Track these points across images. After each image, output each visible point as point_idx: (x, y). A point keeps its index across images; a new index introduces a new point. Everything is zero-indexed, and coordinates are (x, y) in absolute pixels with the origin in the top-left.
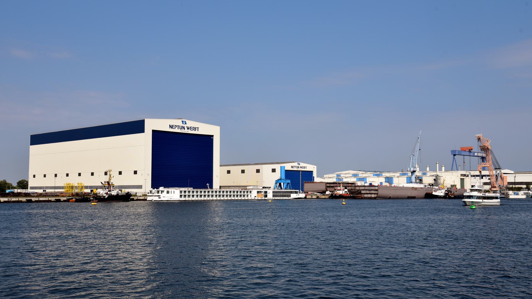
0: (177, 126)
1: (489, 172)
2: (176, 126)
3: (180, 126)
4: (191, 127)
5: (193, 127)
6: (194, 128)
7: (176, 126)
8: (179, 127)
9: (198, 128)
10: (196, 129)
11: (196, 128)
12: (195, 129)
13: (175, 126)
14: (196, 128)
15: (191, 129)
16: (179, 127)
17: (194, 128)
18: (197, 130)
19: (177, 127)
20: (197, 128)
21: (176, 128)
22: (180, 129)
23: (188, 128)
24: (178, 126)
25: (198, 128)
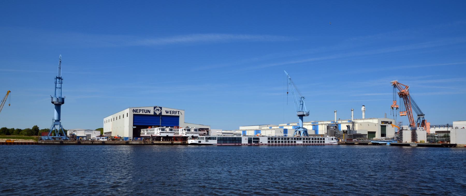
0: (142, 110)
1: (61, 96)
2: (140, 110)
3: (145, 110)
4: (170, 111)
5: (173, 111)
6: (174, 112)
7: (140, 110)
8: (144, 111)
10: (176, 113)
11: (177, 112)
12: (175, 113)
14: (176, 111)
15: (170, 112)
16: (144, 111)
17: (174, 112)
19: (141, 111)
20: (177, 112)
21: (140, 112)
22: (145, 112)
24: (143, 110)
25: (179, 112)
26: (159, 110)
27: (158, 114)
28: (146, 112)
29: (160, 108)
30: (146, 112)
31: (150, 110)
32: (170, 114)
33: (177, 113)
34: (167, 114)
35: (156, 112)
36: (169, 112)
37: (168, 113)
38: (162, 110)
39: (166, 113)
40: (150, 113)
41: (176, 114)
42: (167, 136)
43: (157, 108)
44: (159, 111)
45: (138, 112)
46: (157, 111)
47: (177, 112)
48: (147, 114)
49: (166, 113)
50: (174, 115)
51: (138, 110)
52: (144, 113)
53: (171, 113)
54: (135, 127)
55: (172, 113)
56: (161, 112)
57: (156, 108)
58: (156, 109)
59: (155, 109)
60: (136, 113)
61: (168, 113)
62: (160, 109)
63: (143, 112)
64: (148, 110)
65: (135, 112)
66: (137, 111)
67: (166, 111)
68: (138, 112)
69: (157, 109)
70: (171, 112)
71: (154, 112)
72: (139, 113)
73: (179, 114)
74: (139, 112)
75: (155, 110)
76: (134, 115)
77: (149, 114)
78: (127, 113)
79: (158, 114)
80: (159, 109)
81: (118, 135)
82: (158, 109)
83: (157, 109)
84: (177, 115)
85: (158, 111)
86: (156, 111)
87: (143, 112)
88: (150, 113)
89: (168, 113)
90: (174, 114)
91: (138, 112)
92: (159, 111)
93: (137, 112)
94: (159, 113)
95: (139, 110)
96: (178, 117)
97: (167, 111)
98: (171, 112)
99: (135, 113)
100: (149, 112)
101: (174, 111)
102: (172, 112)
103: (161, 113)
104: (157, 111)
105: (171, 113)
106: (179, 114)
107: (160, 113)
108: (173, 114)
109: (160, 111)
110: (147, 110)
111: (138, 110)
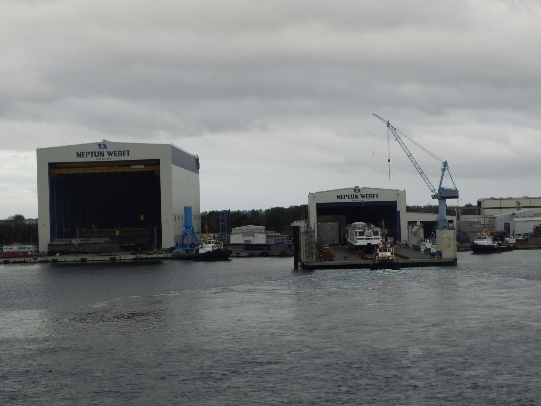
0: (91, 153)
9: (128, 151)
11: (125, 152)
14: (124, 151)
15: (115, 154)
17: (120, 152)
18: (126, 155)
21: (87, 155)
23: (110, 154)
25: (128, 151)
37: (111, 156)
49: (109, 156)
54: (304, 219)
61: (111, 155)
89: (111, 156)
101: (121, 151)
102: (117, 152)
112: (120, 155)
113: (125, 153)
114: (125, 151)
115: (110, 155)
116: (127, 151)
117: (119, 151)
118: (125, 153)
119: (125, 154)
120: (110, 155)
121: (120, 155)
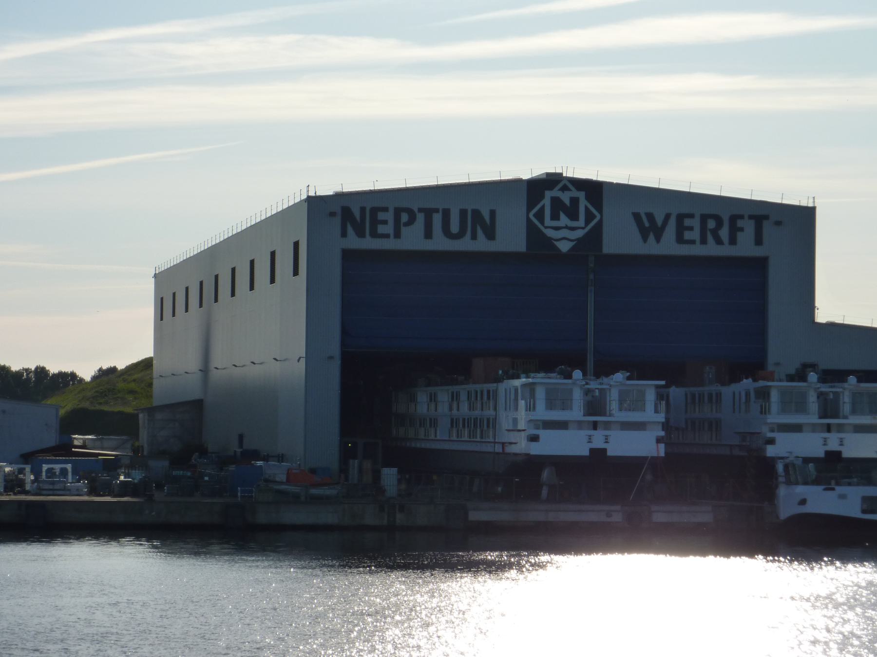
0: (420, 218)
2: (405, 217)
3: (446, 214)
4: (681, 218)
5: (704, 218)
6: (711, 224)
7: (405, 217)
8: (437, 219)
10: (734, 230)
11: (740, 223)
12: (724, 233)
13: (398, 212)
15: (681, 229)
16: (437, 219)
17: (711, 224)
21: (404, 230)
24: (428, 213)
26: (573, 215)
27: (564, 247)
28: (455, 228)
29: (581, 195)
30: (455, 228)
31: (493, 213)
32: (680, 239)
33: (746, 238)
34: (652, 248)
35: (550, 233)
36: (672, 222)
37: (658, 240)
38: (600, 209)
39: (645, 233)
40: (491, 235)
41: (733, 241)
42: (598, 454)
43: (556, 193)
44: (574, 216)
45: (389, 229)
46: (555, 217)
47: (740, 223)
48: (465, 245)
49: (645, 239)
50: (711, 249)
51: (381, 216)
52: (440, 243)
53: (687, 235)
55: (695, 235)
56: (600, 224)
57: (548, 194)
58: (547, 202)
59: (542, 197)
60: (369, 243)
62: (583, 203)
63: (428, 234)
64: (476, 214)
65: (361, 234)
66: (375, 222)
67: (637, 216)
68: (381, 229)
69: (556, 203)
70: (687, 222)
71: (534, 235)
72: (389, 244)
73: (759, 241)
74: (397, 235)
75: (540, 216)
76: (348, 255)
77: (482, 244)
78: (296, 245)
79: (564, 247)
80: (575, 201)
81: (241, 437)
82: (566, 197)
83: (556, 203)
84: (745, 247)
85: (564, 220)
86: (548, 221)
87: (428, 234)
88: (491, 235)
89: (658, 240)
90: (719, 241)
91: (381, 229)
92: (574, 216)
93: (374, 234)
94: (578, 240)
95: (389, 216)
96: (760, 265)
97: (650, 216)
98: (687, 222)
99: (354, 242)
100: (480, 232)
102: (696, 223)
103: (595, 236)
104: (555, 217)
105: (687, 235)
106: (759, 241)
107: (580, 234)
108: (704, 241)
109: (589, 217)
110: (463, 213)
111: (381, 216)
112: (710, 238)
113: (742, 229)
114: (741, 217)
115: (652, 238)
116: (751, 217)
117: (704, 218)
118: (742, 229)
119: (740, 236)
120: (652, 238)
121: (710, 238)
